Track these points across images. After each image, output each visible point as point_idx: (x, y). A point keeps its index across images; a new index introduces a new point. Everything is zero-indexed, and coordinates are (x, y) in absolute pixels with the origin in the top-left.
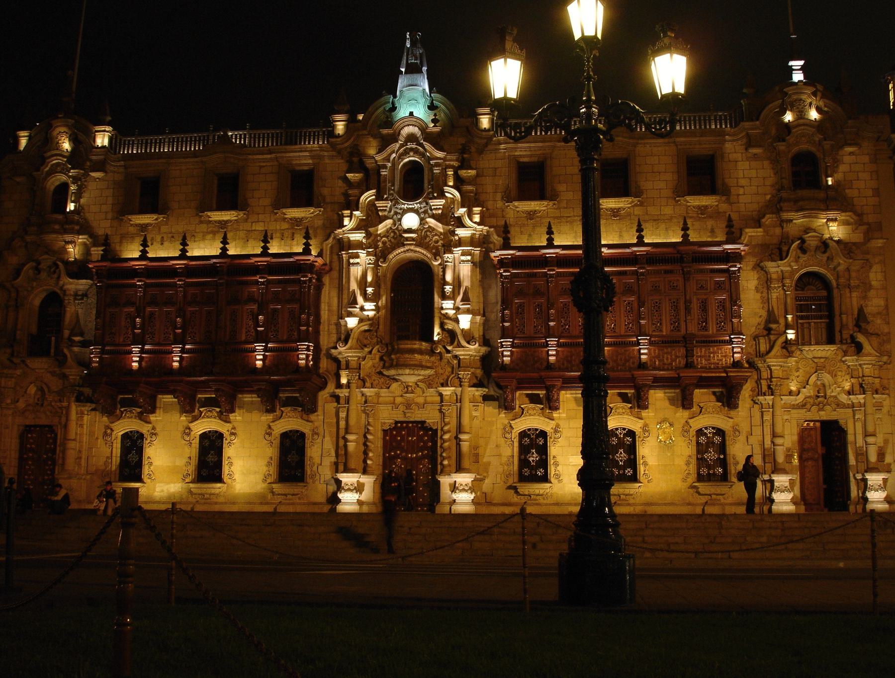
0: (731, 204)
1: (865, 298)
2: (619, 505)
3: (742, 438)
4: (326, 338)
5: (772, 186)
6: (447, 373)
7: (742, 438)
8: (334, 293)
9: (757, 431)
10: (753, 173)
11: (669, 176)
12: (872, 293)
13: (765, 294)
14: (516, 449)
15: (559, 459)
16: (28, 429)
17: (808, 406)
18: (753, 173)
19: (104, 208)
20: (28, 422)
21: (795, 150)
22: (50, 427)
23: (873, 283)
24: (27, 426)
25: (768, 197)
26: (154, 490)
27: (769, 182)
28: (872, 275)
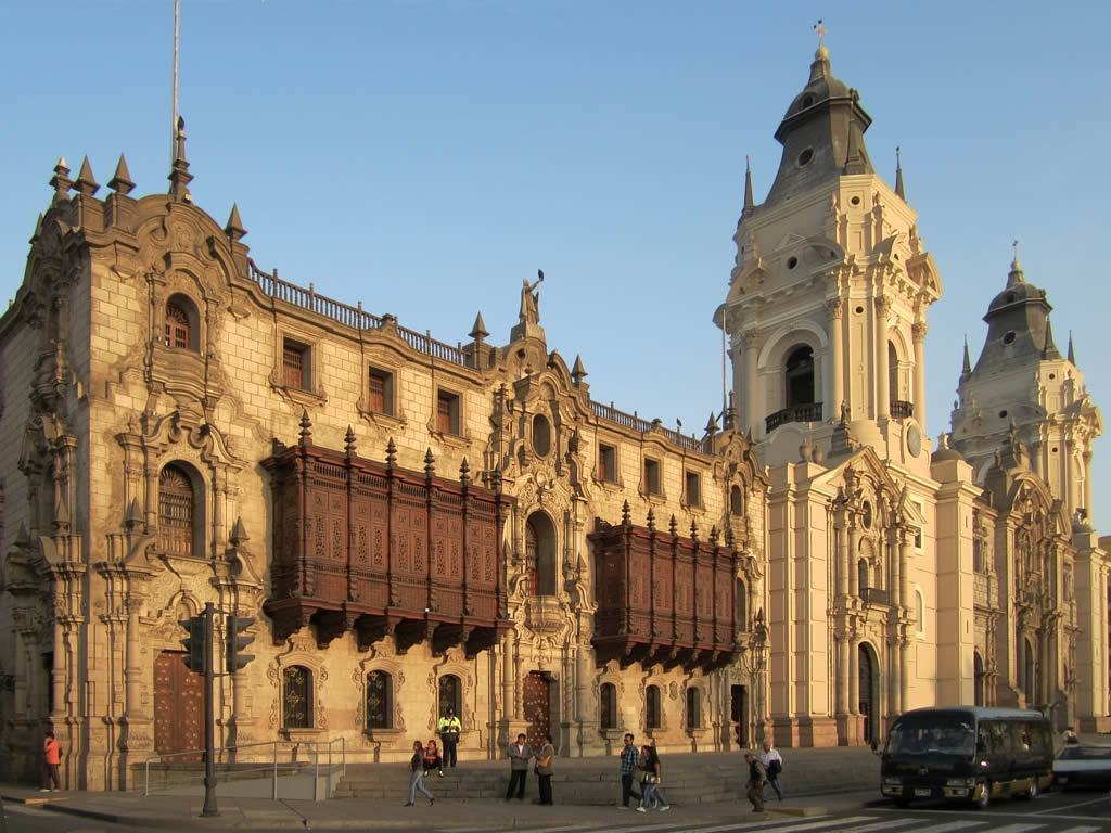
18: (714, 496)
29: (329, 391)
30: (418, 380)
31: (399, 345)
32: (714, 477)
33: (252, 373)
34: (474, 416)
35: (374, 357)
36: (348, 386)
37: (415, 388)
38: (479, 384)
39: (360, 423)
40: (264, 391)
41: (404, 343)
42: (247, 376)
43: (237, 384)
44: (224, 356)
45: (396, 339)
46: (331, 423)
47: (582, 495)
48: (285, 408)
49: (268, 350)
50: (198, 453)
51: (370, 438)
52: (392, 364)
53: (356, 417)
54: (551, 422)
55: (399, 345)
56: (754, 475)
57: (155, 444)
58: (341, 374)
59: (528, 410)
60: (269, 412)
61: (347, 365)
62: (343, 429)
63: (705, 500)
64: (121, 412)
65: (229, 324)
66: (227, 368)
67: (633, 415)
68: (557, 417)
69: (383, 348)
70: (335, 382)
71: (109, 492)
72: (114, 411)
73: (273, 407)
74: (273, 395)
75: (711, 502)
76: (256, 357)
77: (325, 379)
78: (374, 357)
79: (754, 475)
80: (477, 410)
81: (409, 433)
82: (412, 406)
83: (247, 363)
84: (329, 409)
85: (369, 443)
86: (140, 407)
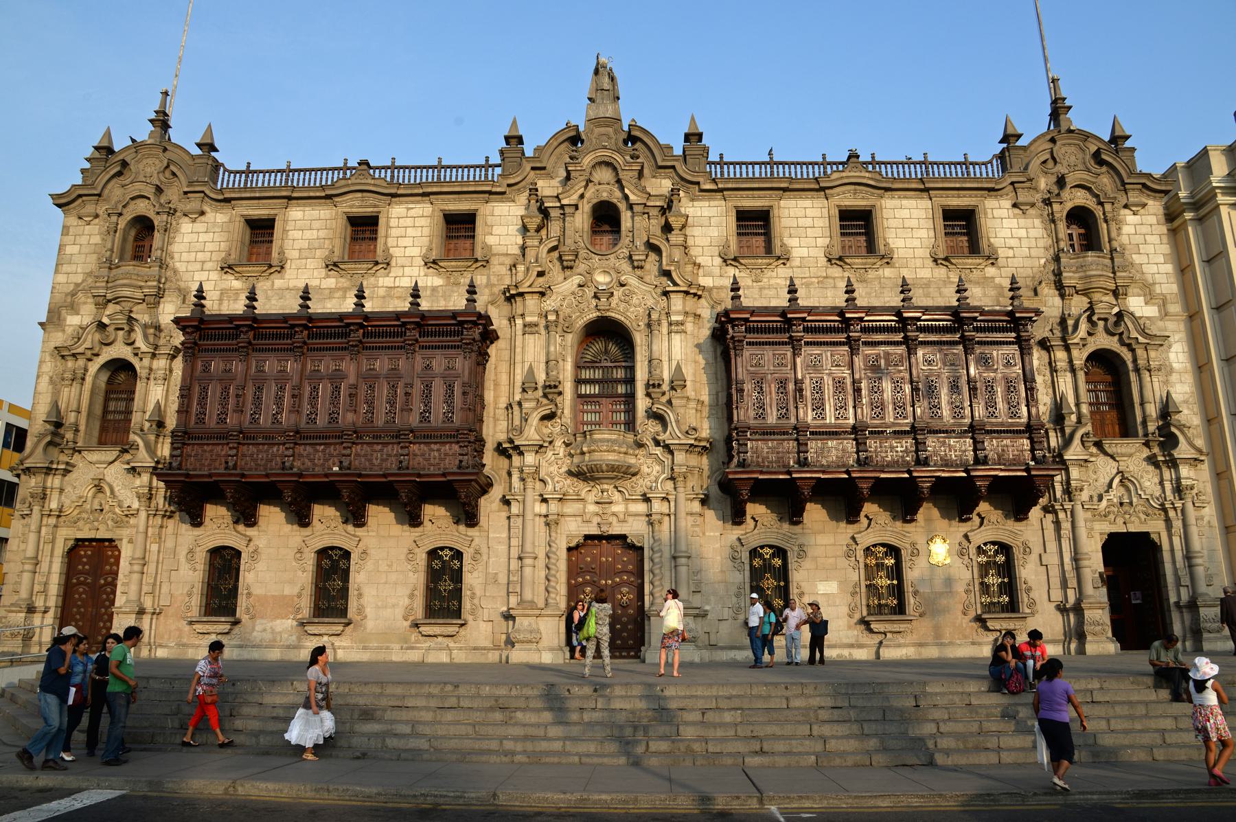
0: (999, 268)
1: (1166, 382)
2: (887, 646)
3: (1034, 557)
4: (491, 425)
5: (1046, 249)
6: (655, 473)
7: (1034, 557)
8: (504, 367)
9: (1052, 546)
10: (1023, 233)
11: (923, 233)
12: (1174, 377)
13: (1048, 377)
14: (747, 573)
15: (806, 587)
16: (79, 542)
17: (1112, 517)
18: (1023, 233)
19: (200, 256)
20: (80, 535)
21: (1069, 206)
22: (111, 540)
23: (1174, 365)
24: (77, 540)
25: (1043, 261)
26: (253, 629)
27: (1041, 243)
28: (1172, 356)
29: (292, 254)
30: (412, 213)
31: (374, 185)
32: (1015, 205)
33: (203, 262)
34: (496, 230)
35: (351, 207)
36: (316, 245)
37: (409, 222)
38: (503, 193)
39: (328, 276)
40: (214, 276)
41: (378, 182)
42: (198, 266)
43: (186, 277)
44: (176, 256)
45: (370, 181)
46: (291, 286)
47: (675, 284)
48: (237, 284)
49: (224, 236)
50: (129, 349)
51: (339, 289)
52: (375, 206)
53: (324, 271)
54: (622, 206)
55: (374, 185)
56: (1124, 184)
57: (80, 350)
58: (308, 234)
59: (565, 202)
60: (218, 293)
61: (316, 224)
62: (295, 289)
63: (996, 242)
64: (69, 330)
65: (186, 226)
66: (178, 265)
67: (821, 160)
68: (626, 197)
69: (359, 195)
70: (297, 245)
71: (49, 400)
72: (64, 331)
73: (223, 286)
74: (225, 277)
75: (1013, 243)
76: (210, 247)
77: (288, 244)
78: (351, 207)
79: (1124, 184)
80: (502, 226)
81: (394, 271)
82: (402, 242)
83: (200, 256)
84: (290, 272)
85: (339, 294)
86: (87, 320)
